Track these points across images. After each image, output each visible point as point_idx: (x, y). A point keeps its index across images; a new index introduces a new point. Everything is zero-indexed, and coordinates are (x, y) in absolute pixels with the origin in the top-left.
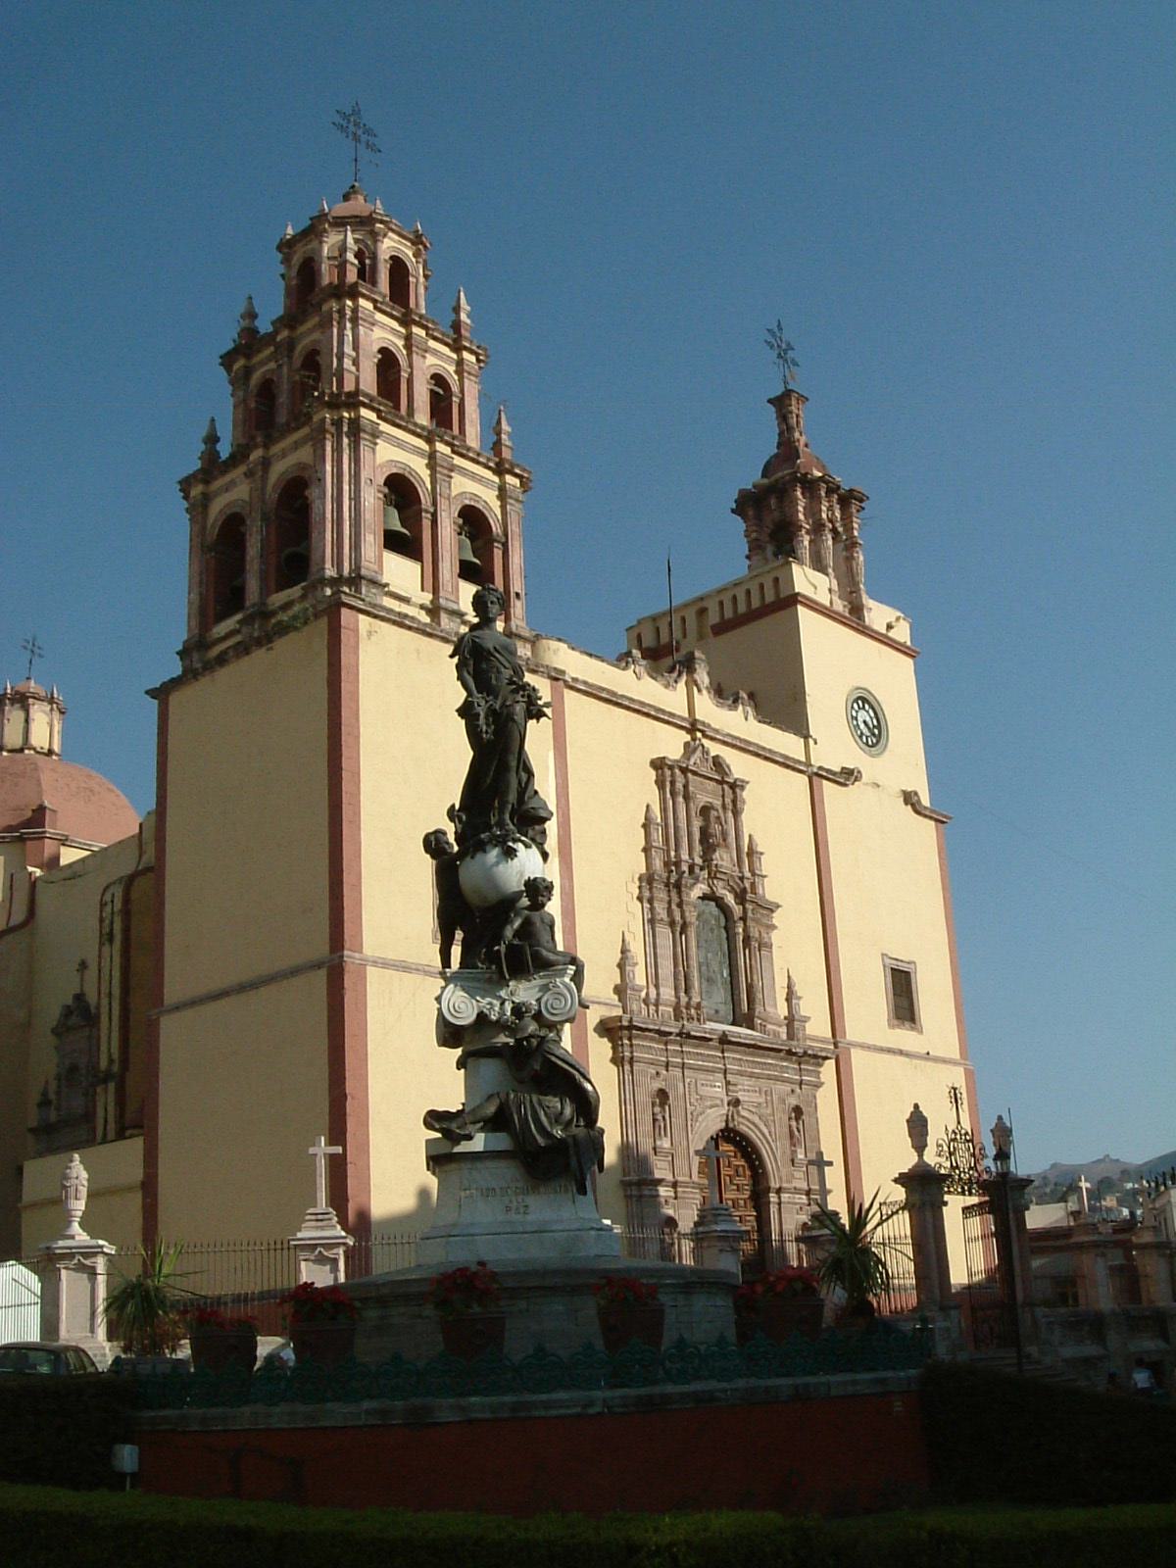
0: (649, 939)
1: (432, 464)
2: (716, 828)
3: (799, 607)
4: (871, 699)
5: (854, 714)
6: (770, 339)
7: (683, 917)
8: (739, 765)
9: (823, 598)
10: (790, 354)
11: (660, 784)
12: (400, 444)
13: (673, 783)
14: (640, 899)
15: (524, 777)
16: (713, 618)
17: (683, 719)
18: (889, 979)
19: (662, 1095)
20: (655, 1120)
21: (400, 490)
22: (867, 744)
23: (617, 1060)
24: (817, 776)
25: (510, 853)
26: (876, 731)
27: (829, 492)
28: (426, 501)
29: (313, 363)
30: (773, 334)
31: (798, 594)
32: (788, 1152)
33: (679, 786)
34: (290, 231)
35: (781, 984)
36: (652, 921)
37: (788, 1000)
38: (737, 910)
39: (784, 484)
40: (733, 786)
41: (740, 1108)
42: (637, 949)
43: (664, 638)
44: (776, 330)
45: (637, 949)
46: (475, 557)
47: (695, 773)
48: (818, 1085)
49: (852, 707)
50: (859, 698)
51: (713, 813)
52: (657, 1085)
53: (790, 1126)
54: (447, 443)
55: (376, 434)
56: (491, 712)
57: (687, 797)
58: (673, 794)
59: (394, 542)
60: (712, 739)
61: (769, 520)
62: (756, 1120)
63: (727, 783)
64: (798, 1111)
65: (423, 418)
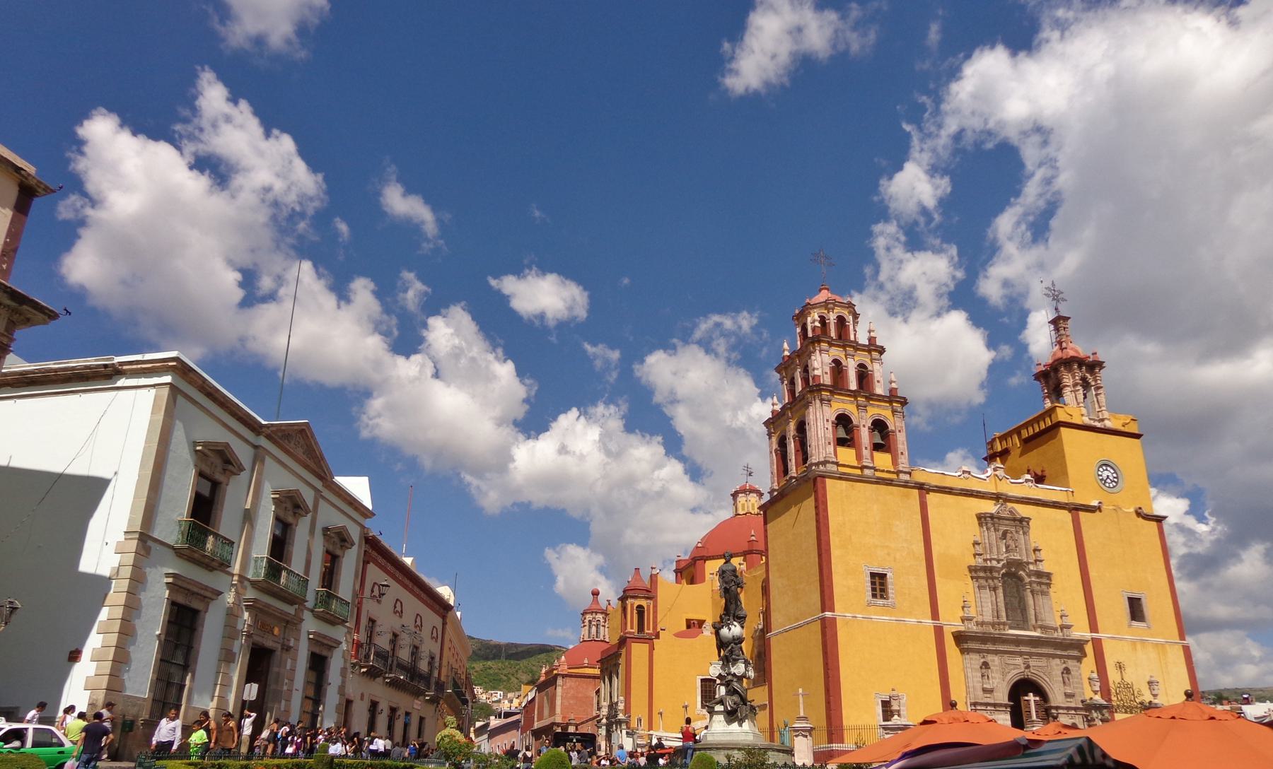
0: (978, 595)
1: (858, 406)
2: (1011, 542)
3: (1063, 430)
4: (1110, 464)
5: (1100, 473)
6: (1047, 292)
7: (995, 584)
8: (1023, 510)
9: (1077, 420)
10: (1061, 296)
11: (981, 525)
12: (843, 402)
13: (986, 524)
14: (972, 578)
15: (739, 603)
16: (1025, 434)
17: (993, 494)
18: (1127, 603)
19: (986, 665)
20: (983, 676)
21: (843, 420)
22: (1109, 487)
23: (963, 651)
24: (1075, 509)
25: (730, 629)
26: (1116, 480)
27: (1080, 367)
28: (855, 422)
29: (806, 370)
30: (1050, 290)
31: (1060, 422)
32: (1062, 689)
33: (989, 525)
34: (797, 312)
35: (1056, 607)
36: (978, 587)
37: (1061, 617)
38: (1027, 580)
39: (1056, 365)
40: (1022, 520)
41: (1031, 669)
42: (971, 598)
43: (1005, 446)
44: (1051, 286)
45: (971, 598)
46: (882, 440)
47: (1000, 518)
48: (1079, 659)
49: (1099, 470)
50: (1099, 468)
51: (1009, 535)
52: (982, 660)
53: (1063, 677)
54: (863, 396)
55: (829, 401)
56: (725, 588)
57: (995, 529)
58: (988, 529)
59: (841, 442)
60: (1010, 501)
61: (1051, 383)
62: (1042, 675)
63: (1018, 520)
64: (1067, 671)
65: (853, 386)
